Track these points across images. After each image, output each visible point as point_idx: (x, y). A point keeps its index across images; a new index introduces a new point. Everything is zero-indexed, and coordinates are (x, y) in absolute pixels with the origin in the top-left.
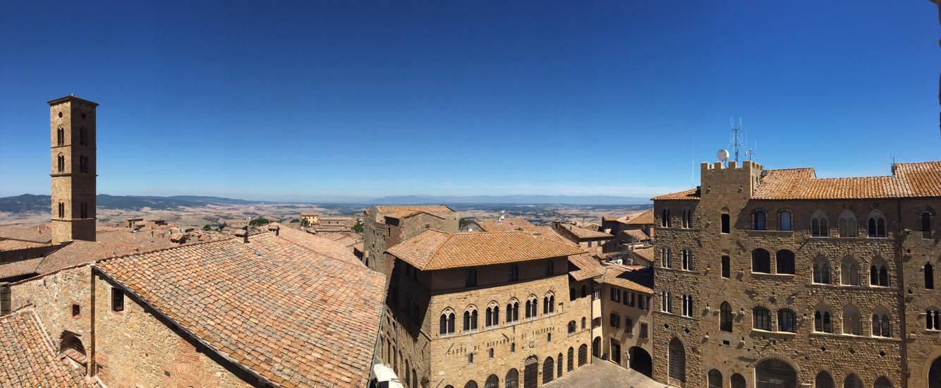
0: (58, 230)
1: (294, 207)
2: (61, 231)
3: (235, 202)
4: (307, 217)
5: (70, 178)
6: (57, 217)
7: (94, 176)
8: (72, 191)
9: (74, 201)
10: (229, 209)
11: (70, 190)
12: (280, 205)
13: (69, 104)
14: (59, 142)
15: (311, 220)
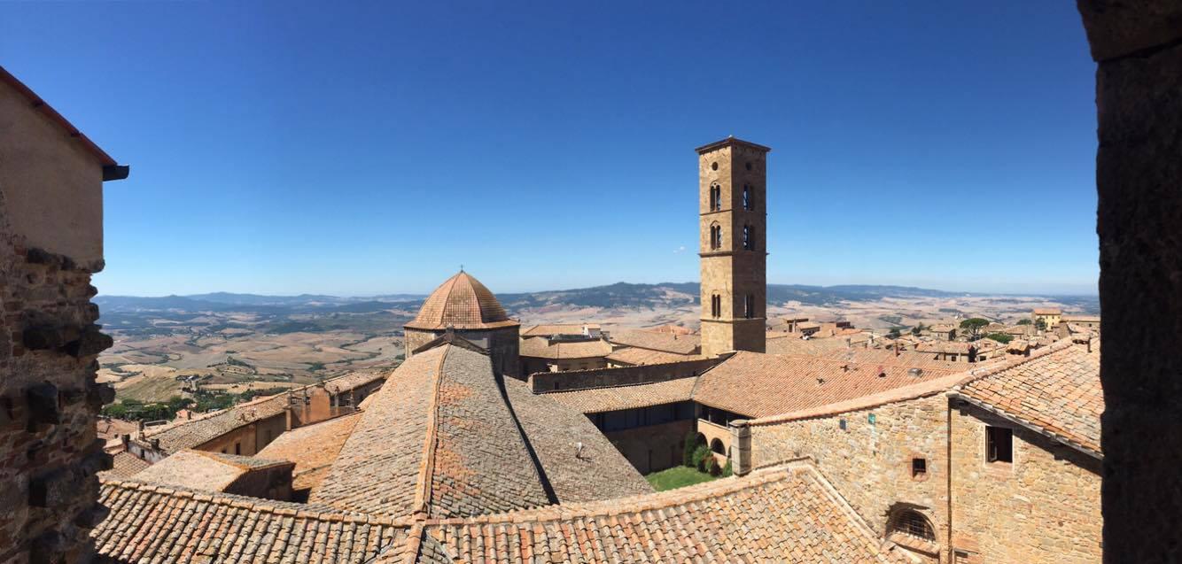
0: (710, 335)
2: (717, 338)
4: (1043, 317)
5: (730, 259)
6: (709, 316)
7: (763, 254)
9: (736, 292)
10: (918, 304)
11: (730, 276)
12: (994, 298)
13: (728, 151)
15: (1049, 321)
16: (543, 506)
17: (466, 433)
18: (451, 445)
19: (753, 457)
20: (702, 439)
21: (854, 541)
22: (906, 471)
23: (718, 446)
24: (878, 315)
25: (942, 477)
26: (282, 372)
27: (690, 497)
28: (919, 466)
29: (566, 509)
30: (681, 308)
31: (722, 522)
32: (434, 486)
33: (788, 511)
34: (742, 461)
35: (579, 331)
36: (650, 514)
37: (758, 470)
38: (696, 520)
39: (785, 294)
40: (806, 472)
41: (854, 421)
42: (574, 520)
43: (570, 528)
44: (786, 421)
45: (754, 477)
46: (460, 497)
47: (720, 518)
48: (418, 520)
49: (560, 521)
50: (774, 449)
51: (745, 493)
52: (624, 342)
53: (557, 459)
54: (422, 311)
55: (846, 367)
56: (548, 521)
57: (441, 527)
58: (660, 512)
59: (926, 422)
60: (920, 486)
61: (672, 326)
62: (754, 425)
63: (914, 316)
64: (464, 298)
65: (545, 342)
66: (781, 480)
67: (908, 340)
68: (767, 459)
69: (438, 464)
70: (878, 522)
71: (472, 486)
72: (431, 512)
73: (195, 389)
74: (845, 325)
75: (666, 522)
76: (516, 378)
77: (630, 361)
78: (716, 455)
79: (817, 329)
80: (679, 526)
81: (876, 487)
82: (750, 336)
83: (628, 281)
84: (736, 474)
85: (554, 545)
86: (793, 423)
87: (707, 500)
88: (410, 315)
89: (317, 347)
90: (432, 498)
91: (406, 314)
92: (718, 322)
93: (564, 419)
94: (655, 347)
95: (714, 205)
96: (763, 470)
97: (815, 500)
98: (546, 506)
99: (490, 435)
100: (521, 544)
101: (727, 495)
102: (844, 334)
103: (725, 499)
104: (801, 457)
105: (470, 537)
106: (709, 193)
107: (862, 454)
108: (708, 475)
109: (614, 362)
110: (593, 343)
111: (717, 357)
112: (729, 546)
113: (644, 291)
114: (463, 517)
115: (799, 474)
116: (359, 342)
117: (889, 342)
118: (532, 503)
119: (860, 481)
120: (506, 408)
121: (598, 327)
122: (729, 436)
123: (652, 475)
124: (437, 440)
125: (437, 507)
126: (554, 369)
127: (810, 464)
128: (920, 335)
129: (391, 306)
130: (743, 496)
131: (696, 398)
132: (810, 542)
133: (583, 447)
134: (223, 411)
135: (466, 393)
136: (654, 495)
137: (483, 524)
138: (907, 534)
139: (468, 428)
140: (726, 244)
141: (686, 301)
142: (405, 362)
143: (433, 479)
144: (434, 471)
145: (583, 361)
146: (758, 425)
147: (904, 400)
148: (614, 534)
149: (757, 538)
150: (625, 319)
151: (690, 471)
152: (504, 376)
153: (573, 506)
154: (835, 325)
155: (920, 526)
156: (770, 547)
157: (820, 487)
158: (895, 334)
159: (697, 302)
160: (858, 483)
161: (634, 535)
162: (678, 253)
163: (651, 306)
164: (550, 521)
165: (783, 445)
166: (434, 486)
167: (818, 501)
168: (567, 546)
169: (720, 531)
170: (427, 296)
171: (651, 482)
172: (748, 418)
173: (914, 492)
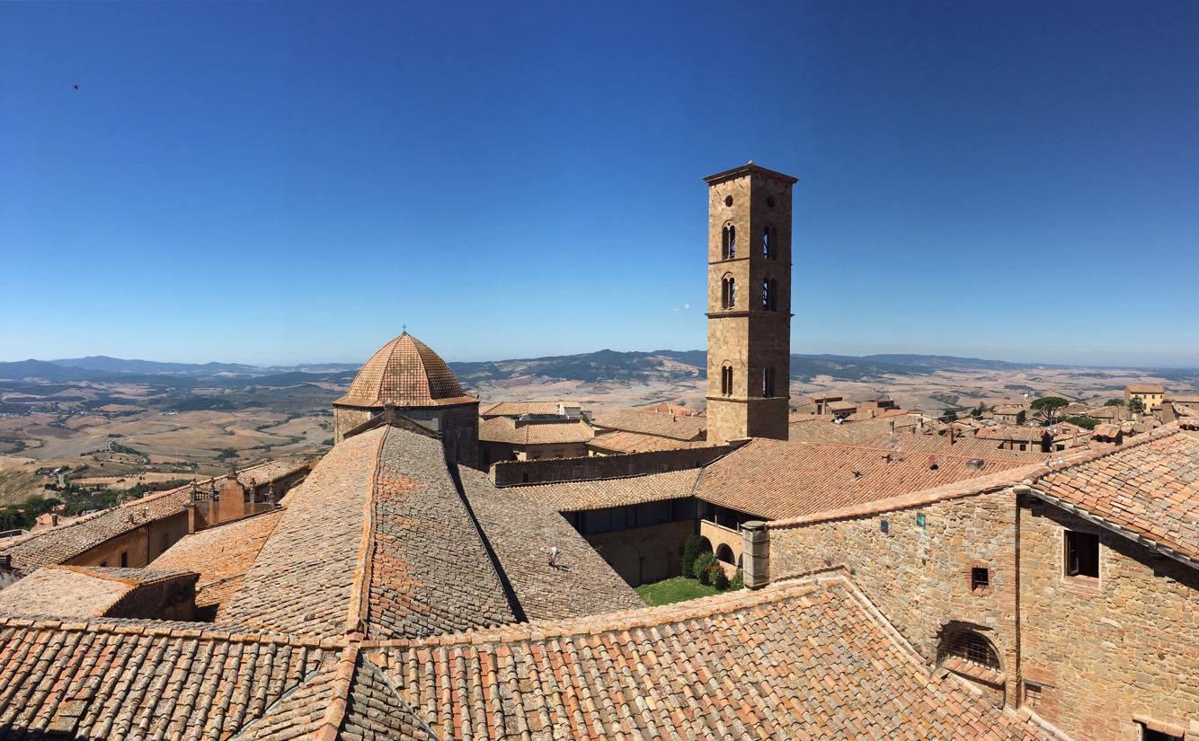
0: (719, 416)
1: (1102, 376)
2: (727, 422)
3: (990, 365)
4: (1142, 396)
5: (745, 321)
6: (718, 393)
7: (787, 315)
8: (750, 346)
9: (752, 363)
11: (746, 342)
12: (1076, 372)
13: (746, 181)
14: (725, 253)
15: (1148, 402)
16: (508, 625)
17: (412, 535)
18: (393, 550)
19: (772, 566)
20: (706, 544)
21: (898, 669)
22: (964, 583)
23: (726, 552)
24: (931, 392)
25: (1009, 592)
27: (690, 613)
28: (980, 577)
29: (537, 628)
30: (683, 383)
31: (730, 644)
32: (371, 600)
33: (817, 631)
34: (755, 571)
35: (552, 410)
36: (640, 633)
37: (778, 583)
38: (697, 641)
39: (815, 366)
40: (839, 585)
41: (899, 522)
42: (547, 640)
43: (543, 650)
44: (815, 522)
45: (771, 591)
46: (404, 614)
47: (727, 640)
48: (351, 641)
49: (530, 642)
50: (799, 556)
51: (761, 609)
52: (610, 425)
54: (356, 384)
55: (888, 457)
56: (516, 641)
57: (382, 650)
58: (654, 630)
59: (989, 523)
60: (982, 602)
61: (670, 405)
62: (773, 528)
63: (973, 395)
64: (411, 367)
65: (512, 423)
66: (808, 595)
67: (966, 424)
68: (790, 569)
69: (377, 573)
70: (927, 645)
71: (419, 601)
72: (368, 632)
73: (63, 486)
74: (888, 405)
75: (660, 642)
76: (474, 468)
78: (722, 564)
79: (854, 410)
80: (677, 647)
81: (925, 604)
82: (769, 418)
84: (748, 587)
85: (522, 670)
86: (824, 525)
87: (712, 617)
88: (341, 389)
90: (370, 615)
91: (336, 388)
92: (729, 400)
93: (534, 518)
94: (649, 431)
95: (728, 252)
96: (783, 583)
97: (850, 618)
98: (512, 625)
99: (441, 538)
100: (481, 670)
101: (736, 611)
102: (887, 416)
103: (734, 616)
104: (833, 566)
105: (418, 662)
106: (721, 235)
107: (908, 562)
108: (712, 589)
109: (596, 449)
110: (571, 425)
111: (727, 444)
112: (738, 672)
114: (407, 638)
115: (831, 587)
116: (279, 423)
117: (943, 426)
118: (494, 620)
119: (907, 596)
120: (461, 504)
121: (577, 405)
122: (740, 542)
123: (643, 588)
124: (376, 544)
125: (376, 626)
126: (522, 457)
127: (845, 575)
128: (982, 418)
129: (317, 377)
130: (758, 613)
131: (699, 494)
132: (844, 669)
133: (557, 553)
134: (103, 512)
135: (411, 486)
136: (645, 610)
137: (432, 647)
138: (965, 660)
139: (413, 529)
140: (741, 301)
141: (689, 375)
142: (335, 449)
143: (370, 592)
144: (372, 581)
145: (559, 447)
146: (779, 527)
147: (961, 497)
148: (597, 656)
149: (775, 664)
150: (612, 395)
151: (690, 583)
152: (459, 465)
153: (545, 624)
154: (876, 404)
155: (981, 650)
156: (791, 676)
157: (856, 603)
158: (950, 416)
159: (703, 375)
160: (903, 599)
161: (621, 658)
162: (677, 312)
163: (644, 380)
164: (518, 642)
165: (811, 552)
166: (371, 600)
167: (853, 620)
168: (538, 672)
169: (728, 655)
170: (361, 365)
171: (641, 595)
172: (765, 520)
173: (973, 609)
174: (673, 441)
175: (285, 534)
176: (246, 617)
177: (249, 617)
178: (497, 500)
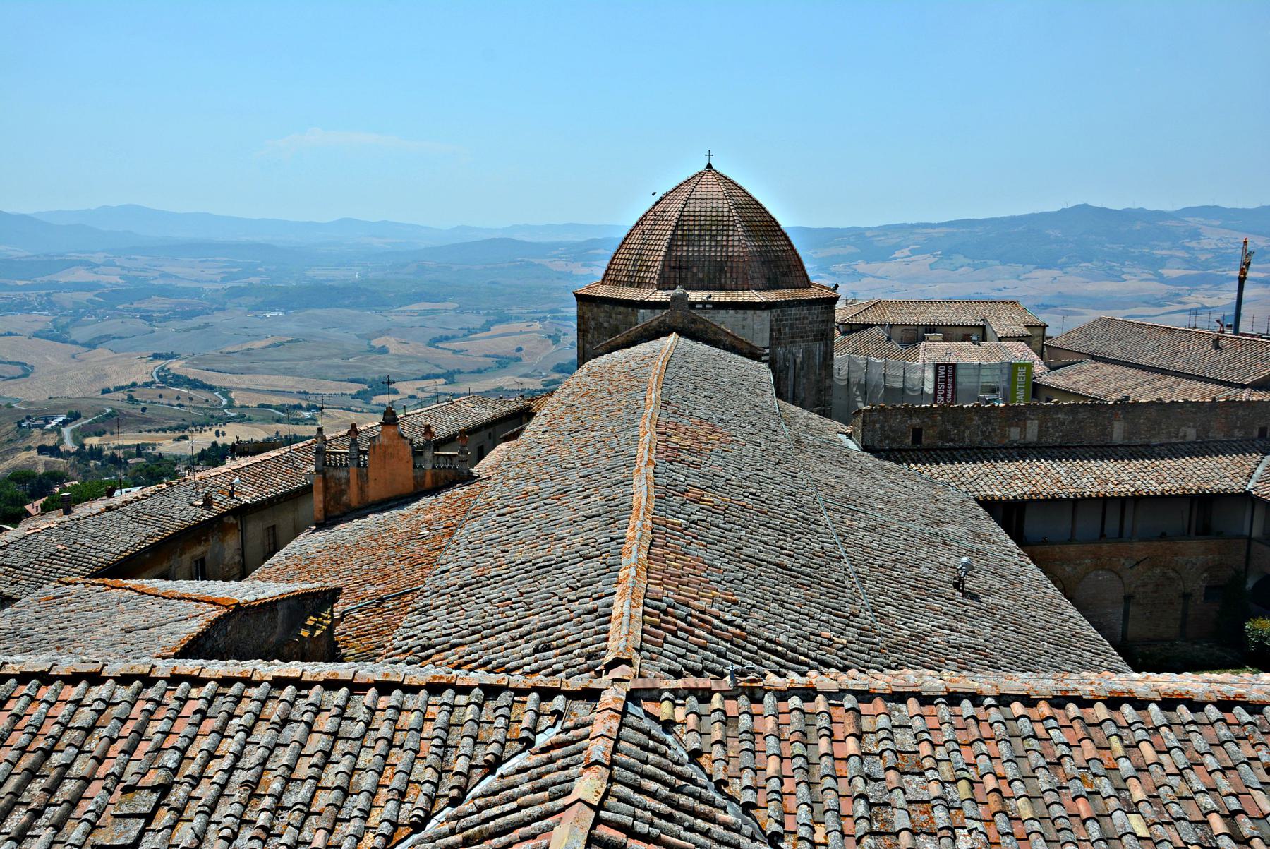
26: (296, 402)
53: (913, 588)
77: (1093, 391)
83: (1096, 202)
89: (377, 343)
113: (1138, 226)
174: (1211, 386)
175: (494, 517)
176: (429, 652)
177: (433, 651)
178: (862, 472)
